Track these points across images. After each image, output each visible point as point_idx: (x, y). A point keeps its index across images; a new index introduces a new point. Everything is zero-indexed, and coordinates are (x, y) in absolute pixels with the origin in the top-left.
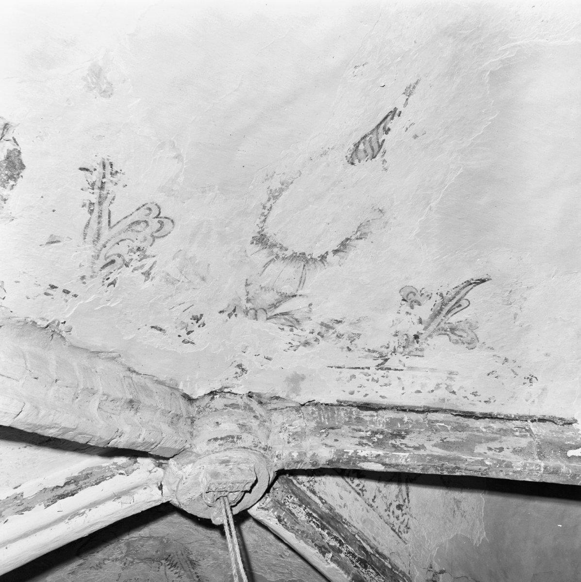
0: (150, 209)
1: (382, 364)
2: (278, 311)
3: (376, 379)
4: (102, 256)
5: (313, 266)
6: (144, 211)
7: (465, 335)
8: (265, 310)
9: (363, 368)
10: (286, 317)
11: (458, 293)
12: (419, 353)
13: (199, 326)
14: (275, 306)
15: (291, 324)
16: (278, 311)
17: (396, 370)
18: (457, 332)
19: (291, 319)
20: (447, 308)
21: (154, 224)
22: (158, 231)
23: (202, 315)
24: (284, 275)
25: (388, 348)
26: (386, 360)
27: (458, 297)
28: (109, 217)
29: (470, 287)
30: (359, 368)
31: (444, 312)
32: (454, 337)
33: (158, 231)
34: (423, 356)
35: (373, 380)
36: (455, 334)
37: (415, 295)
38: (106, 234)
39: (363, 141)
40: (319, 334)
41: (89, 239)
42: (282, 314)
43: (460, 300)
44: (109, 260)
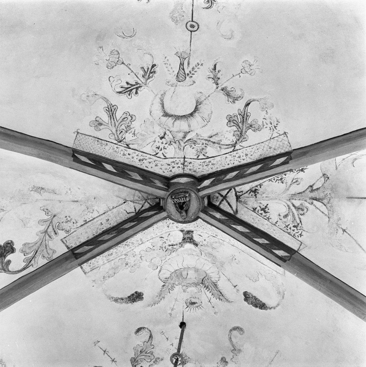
0: (127, 114)
1: (234, 149)
2: (187, 139)
3: (234, 155)
4: (118, 130)
5: (190, 119)
6: (125, 115)
7: (256, 126)
8: (182, 140)
9: (228, 153)
10: (190, 140)
11: (245, 111)
12: (245, 140)
13: (160, 151)
14: (184, 137)
15: (193, 143)
16: (187, 139)
17: (240, 149)
18: (253, 126)
19: (193, 141)
20: (245, 118)
21: (130, 118)
22: (132, 119)
23: (159, 146)
24: (183, 125)
25: (233, 142)
26: (235, 147)
27: (246, 113)
28: (116, 119)
29: (247, 107)
30: (227, 153)
31: (245, 120)
32: (253, 129)
33: (132, 119)
34: (247, 140)
35: (234, 156)
36: (253, 127)
37: (232, 118)
38: (117, 124)
39: (178, 74)
40: (206, 144)
41: (113, 126)
42: (189, 140)
43: (247, 113)
44: (121, 131)
